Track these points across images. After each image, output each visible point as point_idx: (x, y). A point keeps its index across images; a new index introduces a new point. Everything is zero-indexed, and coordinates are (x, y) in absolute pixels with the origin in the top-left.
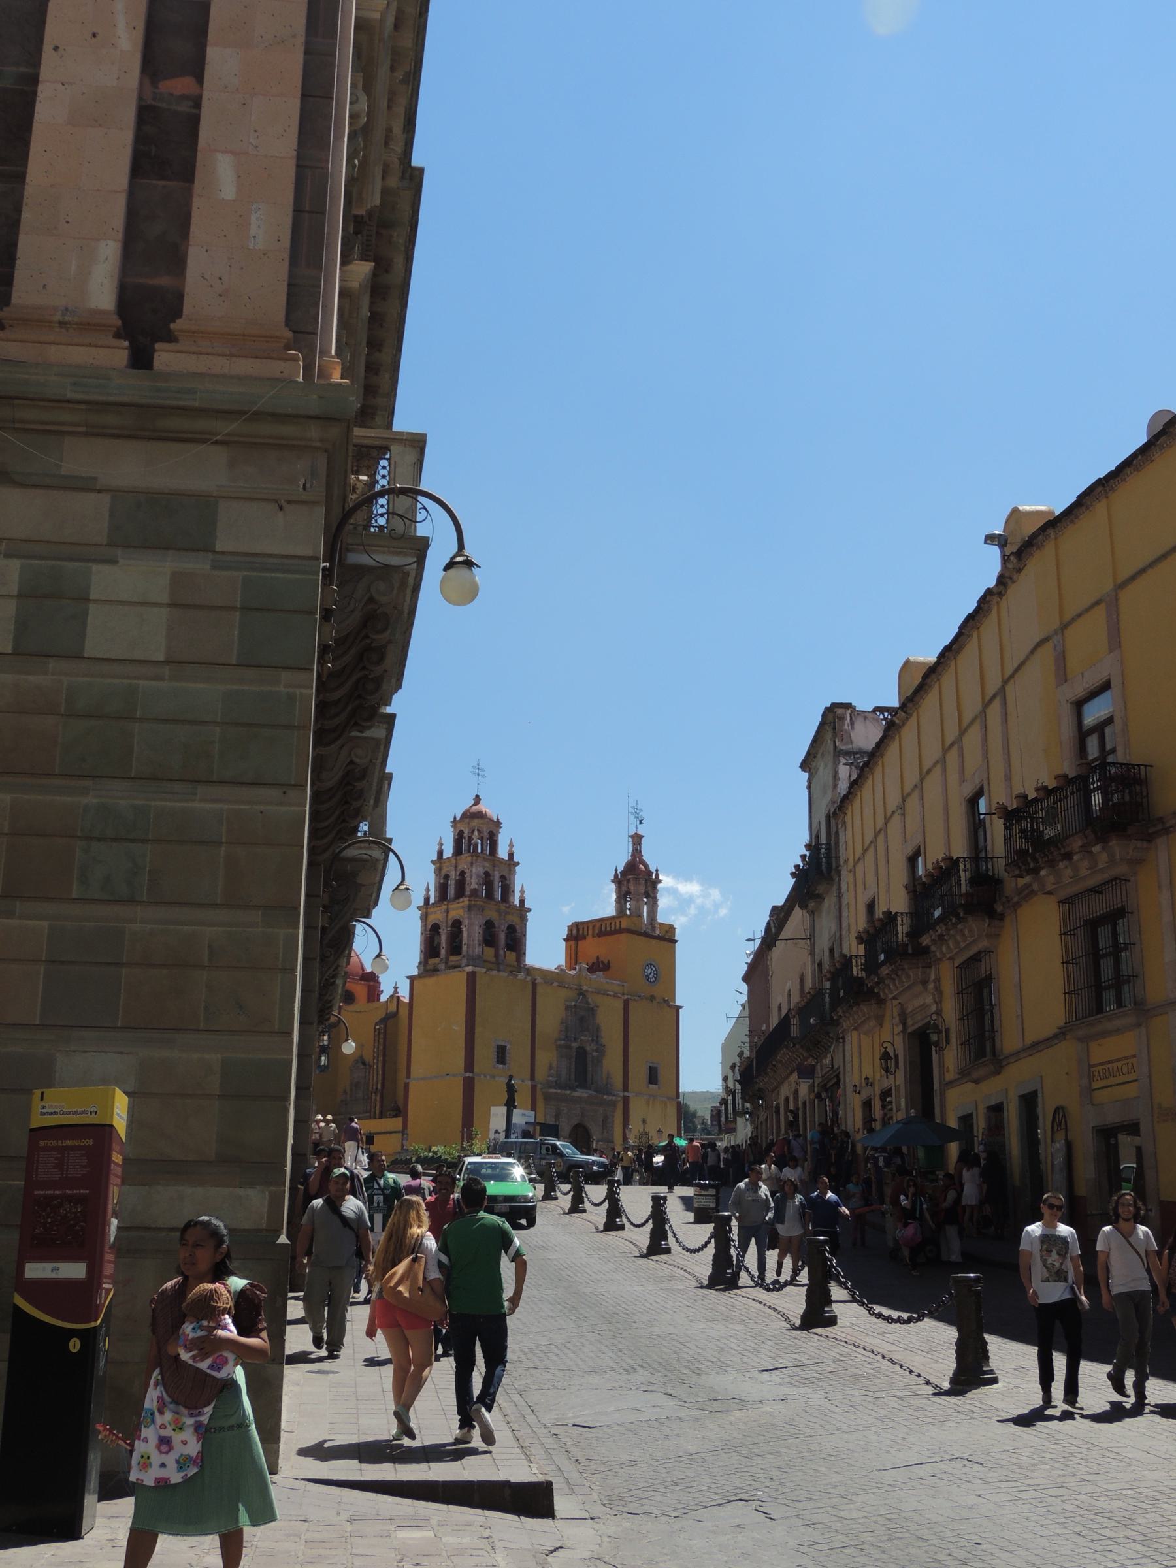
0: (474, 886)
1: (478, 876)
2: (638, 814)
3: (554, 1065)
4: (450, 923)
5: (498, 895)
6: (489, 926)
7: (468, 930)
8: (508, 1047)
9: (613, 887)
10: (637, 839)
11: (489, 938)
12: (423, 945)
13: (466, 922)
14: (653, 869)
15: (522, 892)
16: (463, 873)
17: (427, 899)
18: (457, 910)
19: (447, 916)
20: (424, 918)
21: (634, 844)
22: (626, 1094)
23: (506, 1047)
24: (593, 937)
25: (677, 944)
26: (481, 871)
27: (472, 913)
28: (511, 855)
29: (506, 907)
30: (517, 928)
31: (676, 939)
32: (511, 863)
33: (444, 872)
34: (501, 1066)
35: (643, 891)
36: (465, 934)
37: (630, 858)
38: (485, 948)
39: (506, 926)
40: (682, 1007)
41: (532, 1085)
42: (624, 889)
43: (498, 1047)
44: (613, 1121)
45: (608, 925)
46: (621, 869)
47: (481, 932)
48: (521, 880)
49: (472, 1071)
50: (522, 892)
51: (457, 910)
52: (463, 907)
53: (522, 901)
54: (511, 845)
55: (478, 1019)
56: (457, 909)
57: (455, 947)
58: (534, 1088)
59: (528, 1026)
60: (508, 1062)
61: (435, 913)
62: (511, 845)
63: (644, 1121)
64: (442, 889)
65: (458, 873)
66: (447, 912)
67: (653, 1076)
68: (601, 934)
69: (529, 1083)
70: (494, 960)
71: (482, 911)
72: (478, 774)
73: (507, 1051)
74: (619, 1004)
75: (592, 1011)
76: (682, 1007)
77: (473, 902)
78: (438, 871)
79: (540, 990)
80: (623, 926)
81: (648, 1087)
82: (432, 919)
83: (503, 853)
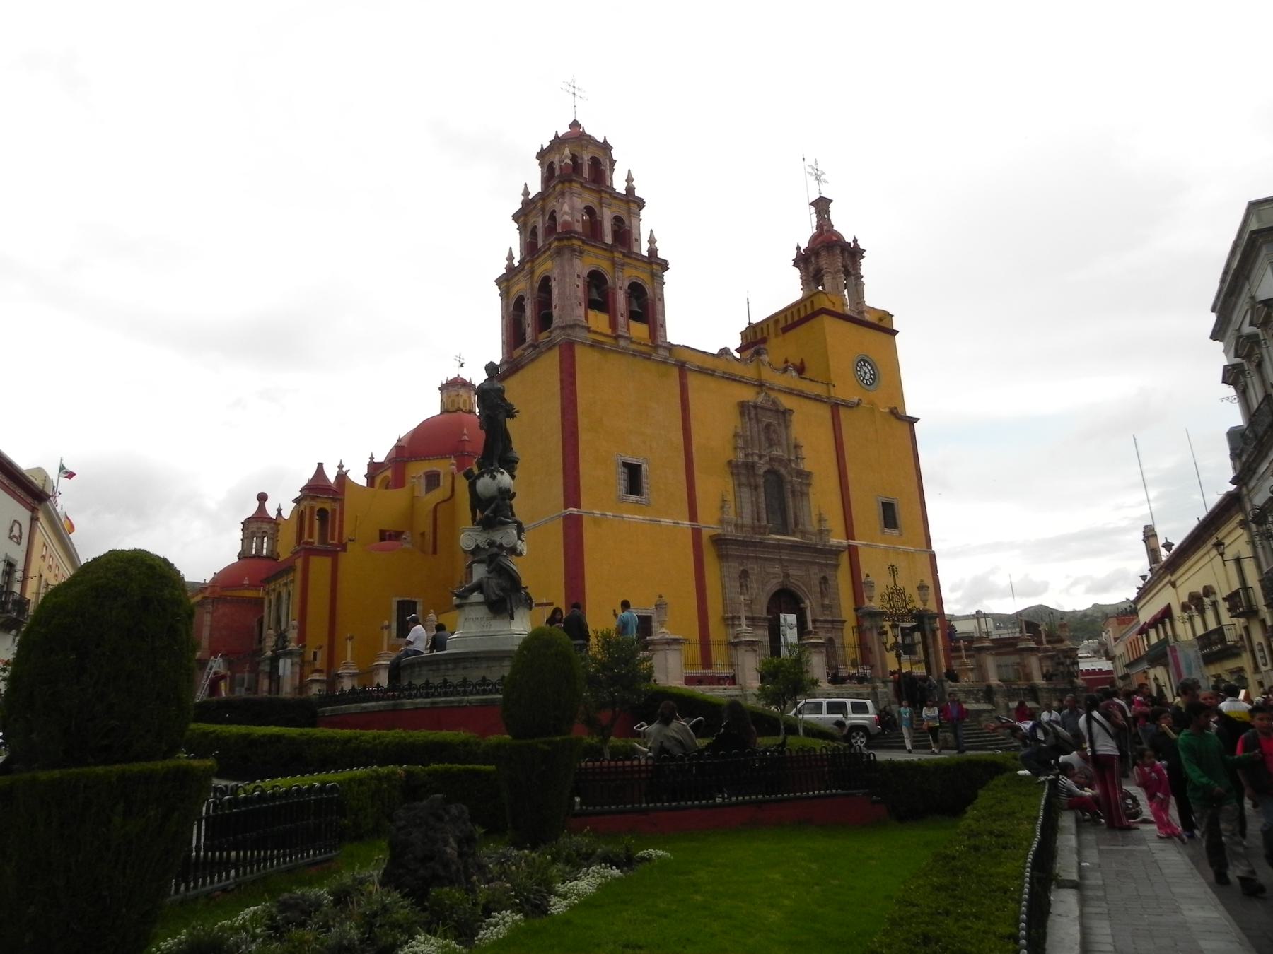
0: (567, 218)
1: (572, 208)
2: (820, 176)
3: (730, 498)
4: (537, 285)
5: (608, 239)
6: (595, 279)
7: (558, 284)
8: (644, 466)
9: (797, 272)
10: (822, 205)
11: (595, 296)
12: (505, 334)
13: (555, 273)
14: (849, 239)
15: (652, 241)
16: (553, 217)
17: (510, 268)
18: (545, 266)
19: (532, 278)
20: (505, 294)
21: (818, 213)
22: (851, 542)
23: (640, 466)
24: (777, 335)
25: (896, 337)
26: (580, 204)
27: (567, 256)
28: (630, 190)
29: (624, 255)
30: (648, 288)
31: (895, 327)
32: (633, 202)
33: (529, 229)
34: (633, 498)
35: (840, 264)
36: (555, 291)
37: (815, 231)
38: (591, 313)
39: (627, 284)
40: (917, 420)
41: (692, 528)
42: (811, 269)
43: (625, 465)
44: (837, 585)
45: (795, 310)
46: (804, 245)
47: (581, 285)
48: (649, 224)
49: (577, 504)
50: (652, 241)
51: (545, 266)
52: (551, 256)
53: (653, 252)
54: (630, 179)
55: (583, 421)
56: (545, 261)
57: (545, 320)
58: (697, 533)
59: (678, 437)
60: (645, 491)
61: (518, 282)
62: (630, 179)
63: (893, 570)
64: (530, 249)
65: (547, 217)
66: (532, 272)
67: (889, 516)
68: (786, 330)
69: (686, 523)
70: (609, 331)
71: (581, 252)
72: (574, 94)
73: (644, 473)
74: (824, 412)
75: (785, 414)
76: (917, 420)
77: (566, 242)
78: (521, 229)
79: (694, 381)
80: (817, 307)
81: (884, 533)
82: (515, 291)
83: (620, 186)
